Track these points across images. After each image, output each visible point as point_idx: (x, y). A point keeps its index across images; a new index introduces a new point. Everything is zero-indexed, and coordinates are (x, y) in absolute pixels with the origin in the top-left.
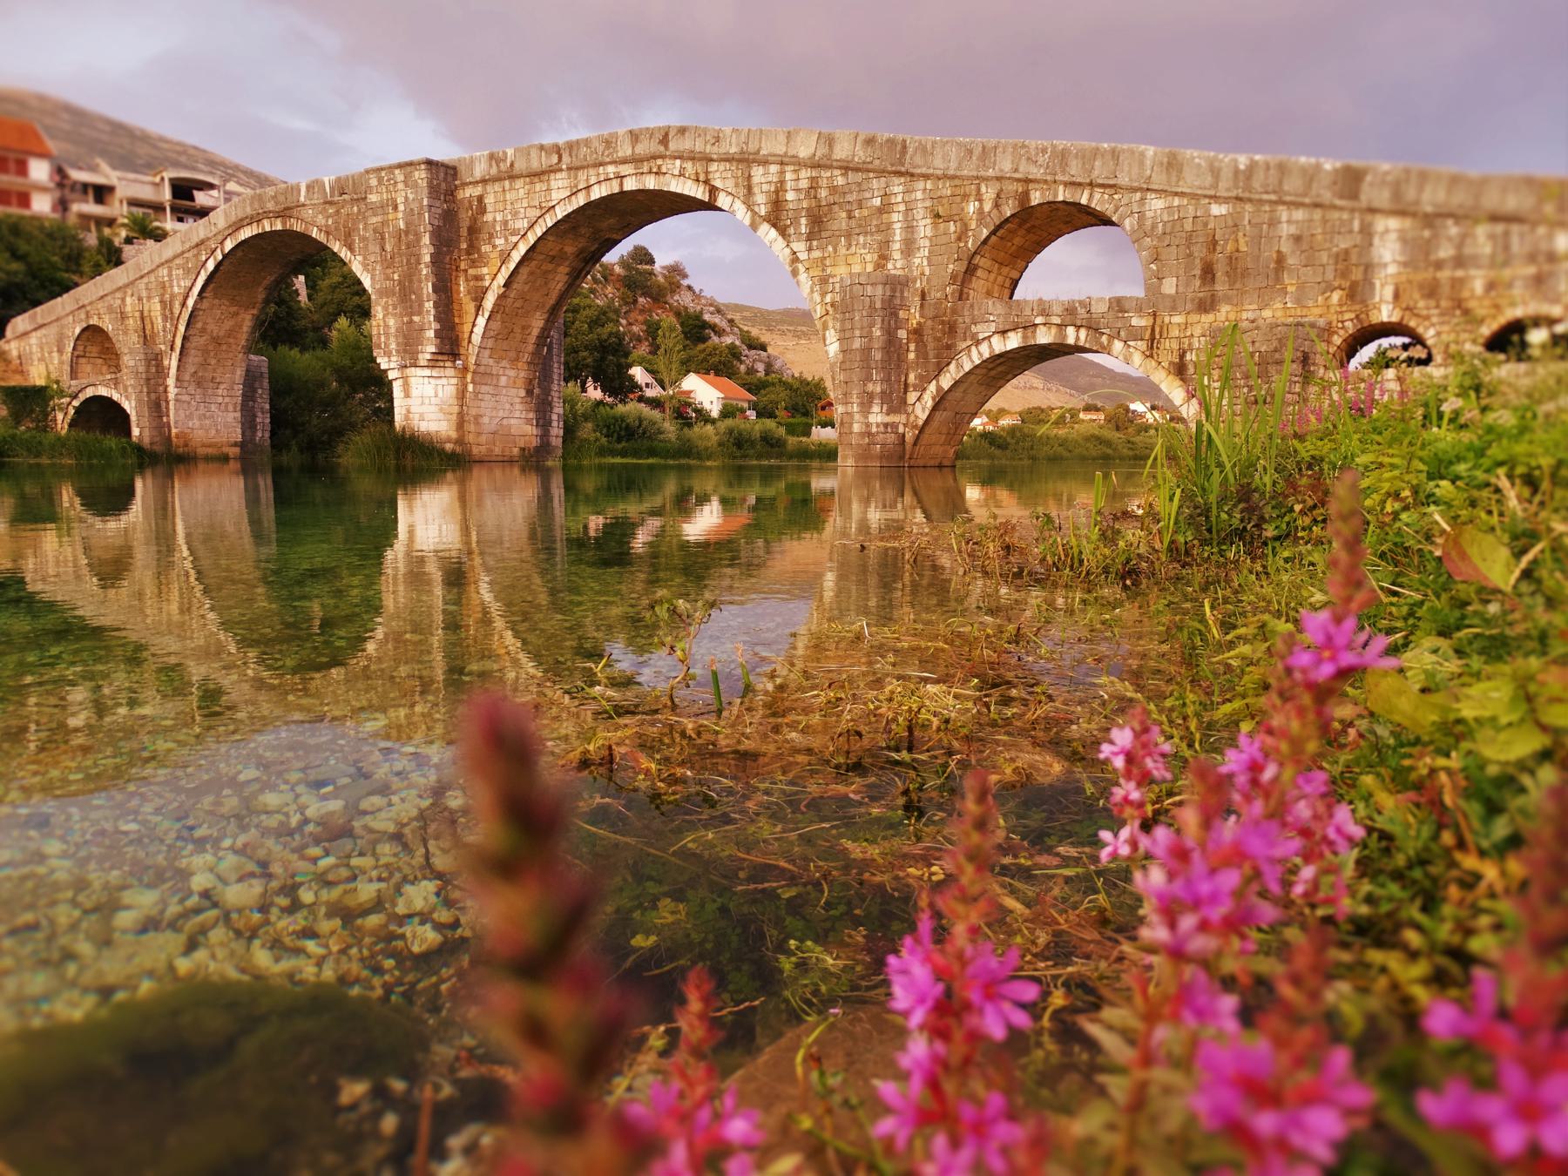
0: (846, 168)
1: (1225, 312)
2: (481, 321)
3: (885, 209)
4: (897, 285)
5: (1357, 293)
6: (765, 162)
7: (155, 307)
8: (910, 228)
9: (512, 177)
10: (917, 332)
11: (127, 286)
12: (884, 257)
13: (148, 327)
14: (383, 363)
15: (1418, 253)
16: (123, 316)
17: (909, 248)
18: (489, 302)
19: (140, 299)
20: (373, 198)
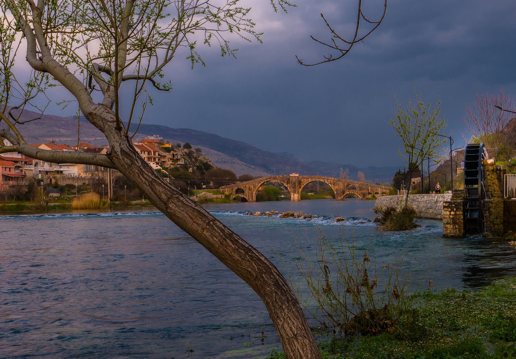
0: (336, 181)
1: (361, 191)
2: (300, 190)
3: (339, 184)
4: (340, 189)
5: (368, 190)
6: (330, 180)
7: (252, 186)
8: (341, 185)
9: (305, 178)
10: (342, 192)
11: (246, 184)
12: (339, 187)
13: (250, 188)
14: (291, 193)
15: (371, 189)
16: (246, 187)
17: (341, 186)
18: (302, 188)
19: (249, 185)
20: (291, 179)
